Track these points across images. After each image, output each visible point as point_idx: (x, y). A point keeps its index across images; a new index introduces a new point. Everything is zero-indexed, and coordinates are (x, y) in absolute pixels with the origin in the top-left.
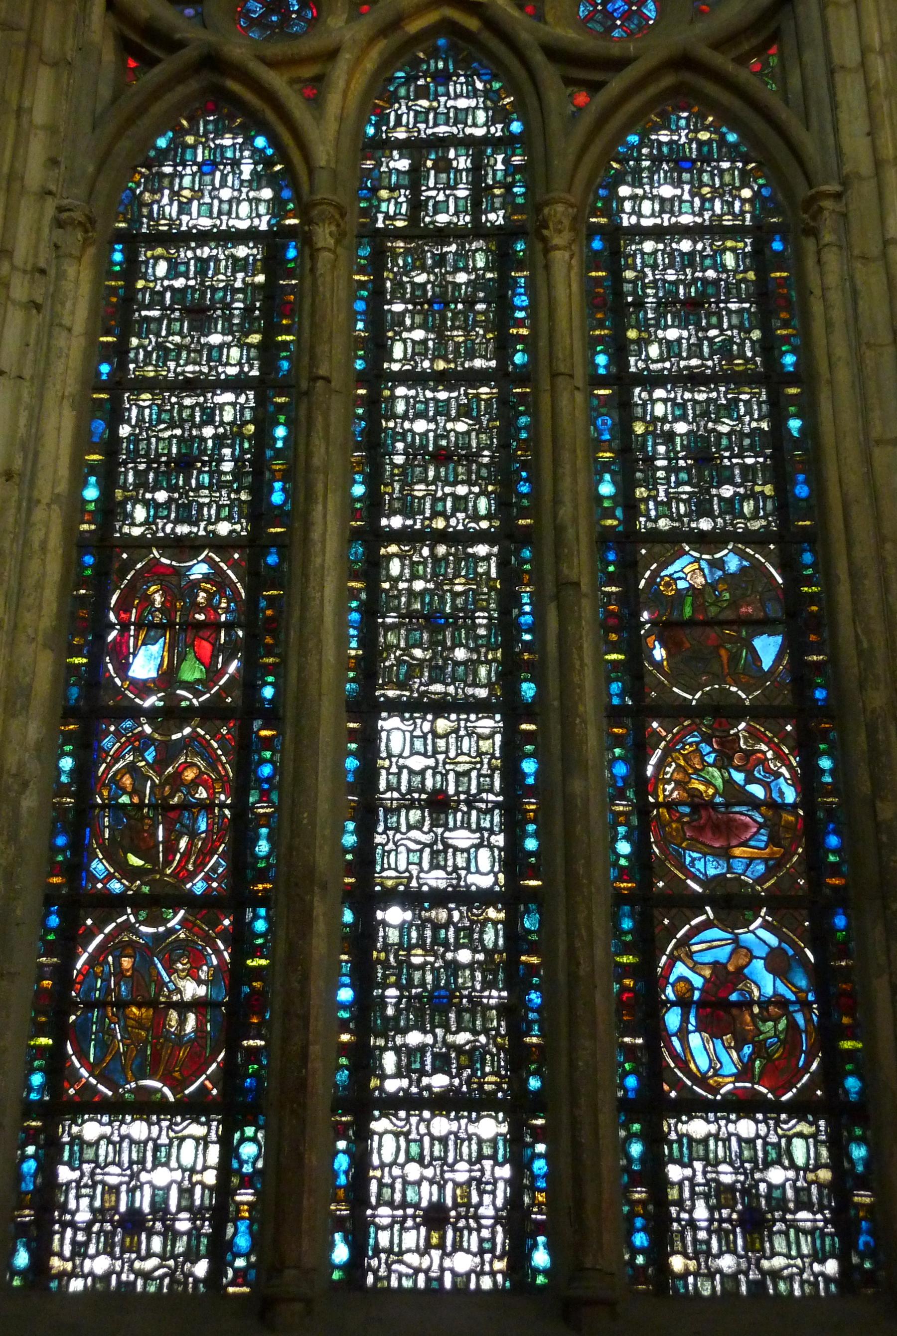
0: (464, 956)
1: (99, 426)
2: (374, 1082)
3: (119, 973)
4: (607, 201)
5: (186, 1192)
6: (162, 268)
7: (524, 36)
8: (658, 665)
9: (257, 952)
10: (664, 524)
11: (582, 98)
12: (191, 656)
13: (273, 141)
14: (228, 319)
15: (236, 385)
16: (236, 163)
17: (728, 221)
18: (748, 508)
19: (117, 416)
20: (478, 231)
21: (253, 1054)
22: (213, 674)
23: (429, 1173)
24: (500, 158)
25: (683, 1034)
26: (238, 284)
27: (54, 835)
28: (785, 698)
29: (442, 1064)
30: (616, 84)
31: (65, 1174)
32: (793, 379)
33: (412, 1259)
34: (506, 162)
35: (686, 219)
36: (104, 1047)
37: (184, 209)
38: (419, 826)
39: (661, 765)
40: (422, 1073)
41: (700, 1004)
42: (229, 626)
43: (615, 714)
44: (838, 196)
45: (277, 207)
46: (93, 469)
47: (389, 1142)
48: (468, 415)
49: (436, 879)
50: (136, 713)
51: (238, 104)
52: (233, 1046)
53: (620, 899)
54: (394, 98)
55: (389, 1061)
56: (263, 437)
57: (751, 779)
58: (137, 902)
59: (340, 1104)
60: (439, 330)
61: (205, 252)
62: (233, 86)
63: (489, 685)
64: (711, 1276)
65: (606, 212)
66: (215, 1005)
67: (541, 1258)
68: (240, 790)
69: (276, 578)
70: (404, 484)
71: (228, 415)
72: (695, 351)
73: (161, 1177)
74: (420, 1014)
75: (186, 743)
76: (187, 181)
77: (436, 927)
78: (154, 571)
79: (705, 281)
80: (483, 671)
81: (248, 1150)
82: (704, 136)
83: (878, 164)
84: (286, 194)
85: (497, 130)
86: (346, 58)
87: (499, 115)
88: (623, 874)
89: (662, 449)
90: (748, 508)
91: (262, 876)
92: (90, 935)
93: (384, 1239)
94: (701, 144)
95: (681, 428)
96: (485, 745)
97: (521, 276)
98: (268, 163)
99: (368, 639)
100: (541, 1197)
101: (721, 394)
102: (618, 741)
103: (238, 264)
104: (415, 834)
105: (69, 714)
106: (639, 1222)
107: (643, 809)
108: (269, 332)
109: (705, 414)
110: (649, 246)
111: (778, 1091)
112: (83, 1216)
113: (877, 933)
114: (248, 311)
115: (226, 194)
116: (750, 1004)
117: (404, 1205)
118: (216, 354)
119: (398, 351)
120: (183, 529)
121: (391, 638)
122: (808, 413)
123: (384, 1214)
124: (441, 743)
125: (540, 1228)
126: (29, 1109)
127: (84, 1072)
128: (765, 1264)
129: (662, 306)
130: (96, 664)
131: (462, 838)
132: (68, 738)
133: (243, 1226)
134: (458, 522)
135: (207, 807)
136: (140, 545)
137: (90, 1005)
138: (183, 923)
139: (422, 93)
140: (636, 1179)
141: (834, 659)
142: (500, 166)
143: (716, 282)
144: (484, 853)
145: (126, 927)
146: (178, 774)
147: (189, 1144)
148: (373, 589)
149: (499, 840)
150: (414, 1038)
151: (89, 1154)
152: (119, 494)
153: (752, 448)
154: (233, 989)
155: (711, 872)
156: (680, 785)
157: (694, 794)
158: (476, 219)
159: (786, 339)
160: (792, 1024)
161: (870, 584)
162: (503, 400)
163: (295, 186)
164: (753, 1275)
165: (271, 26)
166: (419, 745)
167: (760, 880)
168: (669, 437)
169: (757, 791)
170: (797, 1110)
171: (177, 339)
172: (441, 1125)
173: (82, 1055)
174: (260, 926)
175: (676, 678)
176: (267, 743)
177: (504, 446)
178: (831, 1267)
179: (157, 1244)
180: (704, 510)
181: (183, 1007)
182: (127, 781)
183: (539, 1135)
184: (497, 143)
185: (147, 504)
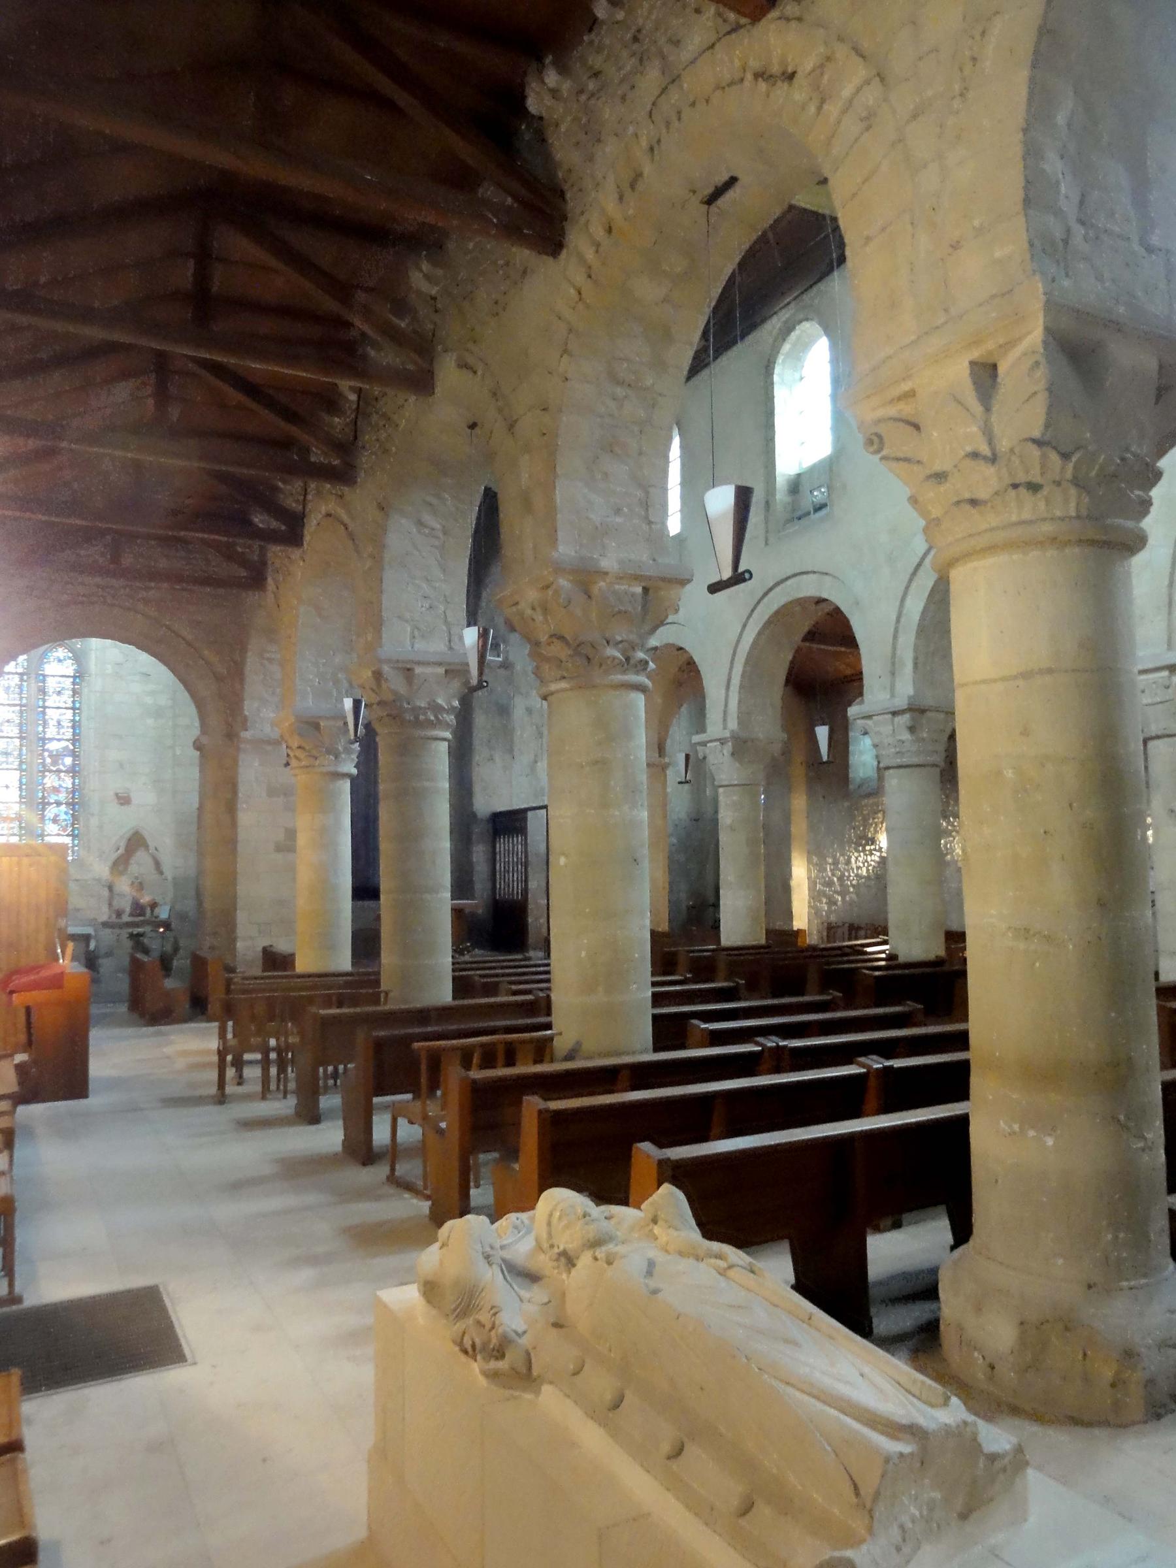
18: (66, 734)
20: (16, 673)
32: (78, 709)
43: (40, 772)
82: (66, 654)
101: (64, 711)
169: (64, 785)
170: (67, 835)
180: (59, 734)
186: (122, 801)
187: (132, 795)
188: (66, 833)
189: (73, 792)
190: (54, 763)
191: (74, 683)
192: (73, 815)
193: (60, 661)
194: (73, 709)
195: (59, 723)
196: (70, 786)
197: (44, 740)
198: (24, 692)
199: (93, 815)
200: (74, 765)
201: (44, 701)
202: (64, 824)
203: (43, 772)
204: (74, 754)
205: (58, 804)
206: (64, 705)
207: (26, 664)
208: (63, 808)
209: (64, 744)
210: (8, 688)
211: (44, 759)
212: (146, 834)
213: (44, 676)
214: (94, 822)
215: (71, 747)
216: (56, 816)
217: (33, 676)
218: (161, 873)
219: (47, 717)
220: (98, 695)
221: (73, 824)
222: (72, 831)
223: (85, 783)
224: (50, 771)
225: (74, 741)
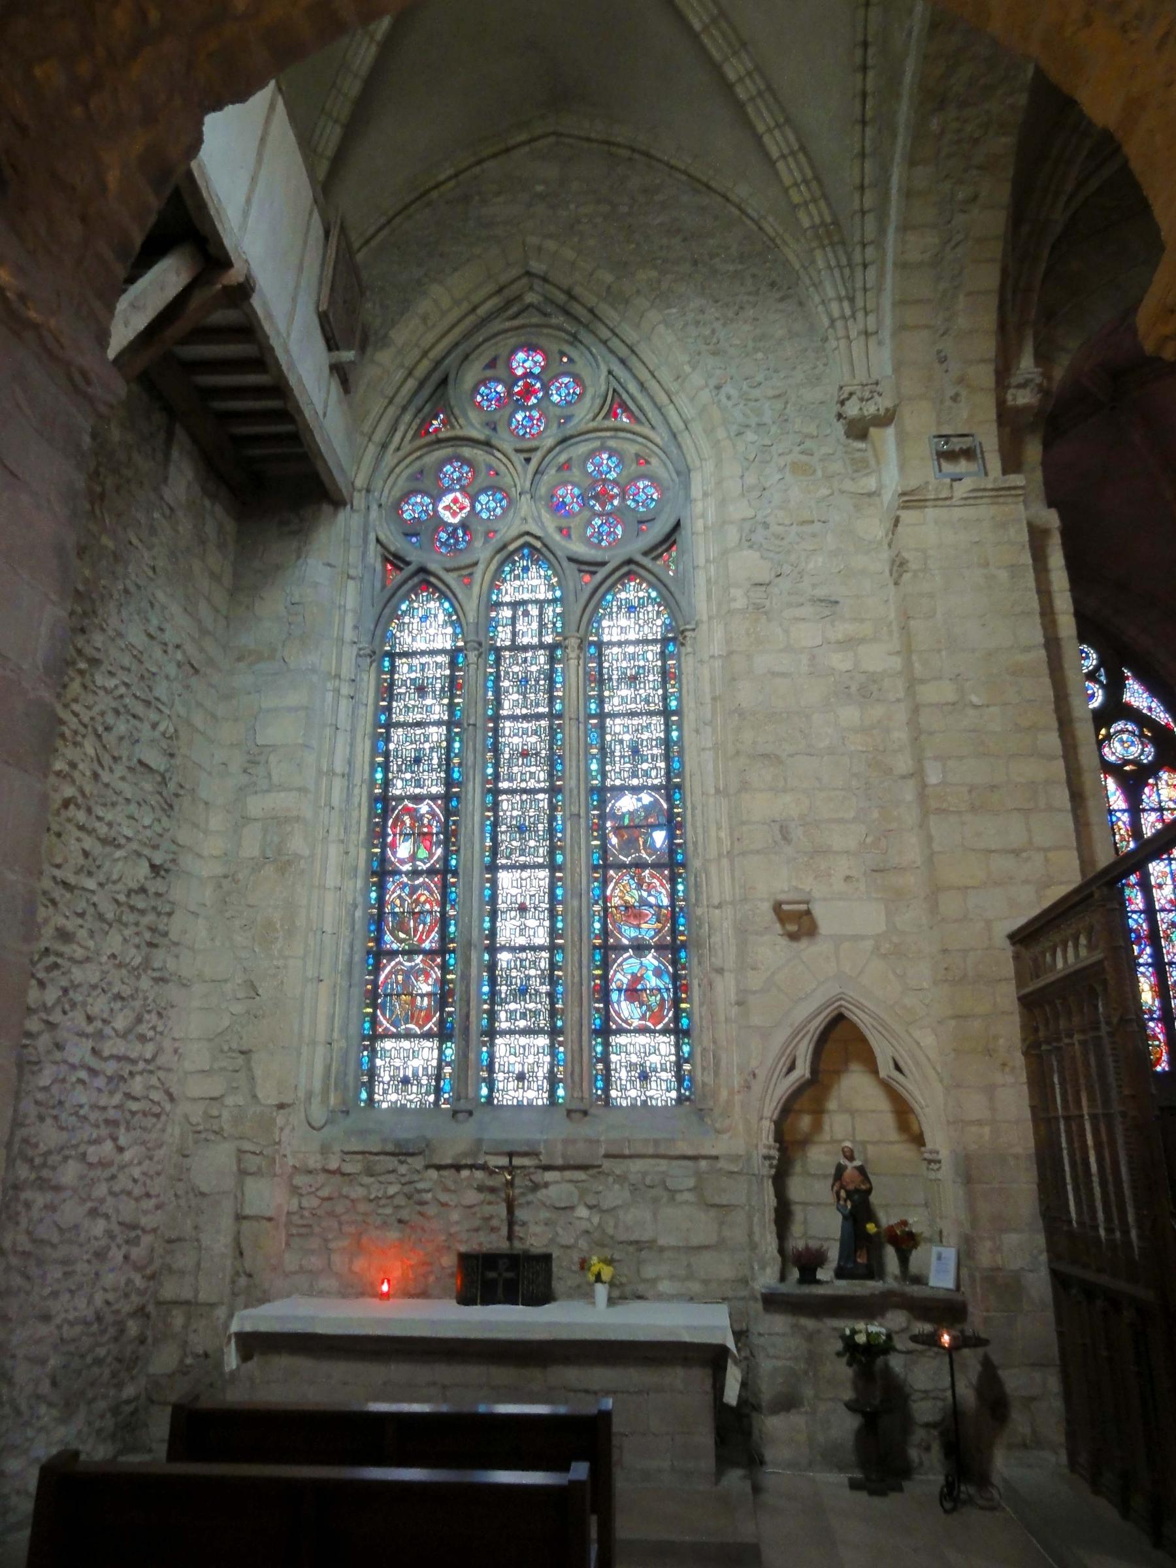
0: (532, 972)
1: (381, 744)
2: (497, 1024)
3: (397, 982)
4: (597, 629)
5: (425, 1069)
6: (405, 668)
7: (559, 553)
8: (614, 846)
9: (451, 972)
10: (618, 783)
11: (587, 577)
12: (422, 847)
13: (452, 605)
14: (434, 692)
15: (438, 723)
16: (436, 616)
17: (650, 637)
18: (654, 773)
19: (388, 740)
20: (541, 646)
21: (450, 1014)
22: (431, 855)
23: (518, 1059)
24: (551, 609)
25: (619, 1002)
26: (438, 675)
27: (369, 924)
28: (665, 859)
29: (523, 1016)
30: (602, 572)
31: (379, 1062)
32: (674, 713)
33: (512, 1093)
34: (554, 611)
35: (632, 636)
36: (392, 1012)
37: (414, 639)
38: (514, 918)
39: (614, 889)
40: (516, 1020)
41: (626, 990)
42: (437, 834)
43: (595, 868)
44: (693, 630)
45: (455, 636)
46: (379, 765)
47: (503, 1047)
48: (536, 734)
49: (521, 941)
50: (399, 873)
51: (436, 589)
52: (442, 1011)
53: (595, 947)
54: (504, 581)
55: (503, 1015)
56: (449, 749)
57: (649, 895)
58: (403, 953)
59: (484, 1033)
60: (524, 695)
61: (424, 660)
62: (432, 579)
63: (544, 857)
64: (626, 1098)
65: (597, 634)
66: (435, 994)
67: (561, 1092)
68: (443, 905)
69: (456, 813)
70: (509, 767)
71: (435, 738)
72: (634, 700)
73: (416, 1063)
74: (515, 996)
75: (420, 886)
76: (415, 626)
77: (521, 961)
78: (407, 810)
79: (639, 667)
80: (541, 850)
81: (448, 1052)
82: (641, 594)
83: (710, 618)
84: (458, 630)
85: (550, 596)
86: (481, 566)
87: (551, 588)
88: (597, 937)
89: (618, 747)
90: (654, 773)
91: (452, 941)
92: (385, 966)
93: (501, 1086)
94: (639, 599)
95: (627, 737)
96: (542, 883)
97: (559, 667)
98: (450, 616)
99: (494, 839)
100: (561, 1068)
101: (644, 721)
102: (596, 879)
103: (438, 666)
104: (513, 922)
105: (374, 873)
106: (599, 1077)
107: (605, 909)
108: (452, 697)
109: (637, 730)
110: (615, 650)
111: (655, 1025)
112: (387, 1079)
113: (695, 961)
114: (443, 688)
115: (432, 631)
116: (645, 990)
117: (509, 1072)
118: (429, 709)
119: (506, 704)
120: (417, 791)
121: (504, 837)
122: (680, 729)
123: (500, 1076)
124: (524, 883)
125: (561, 1080)
126: (364, 1038)
127: (385, 1022)
128: (648, 1094)
129: (619, 680)
130: (383, 852)
131: (531, 923)
132: (374, 884)
133: (447, 1081)
134: (532, 784)
135: (431, 912)
136: (400, 799)
137: (386, 995)
138: (422, 961)
139: (517, 577)
140: (599, 1061)
141: (685, 843)
142: (551, 614)
143: (644, 667)
144: (541, 929)
145: (400, 963)
146: (418, 899)
147: (426, 1050)
148: (496, 816)
149: (547, 923)
150: (513, 1006)
151: (388, 1054)
152: (390, 775)
153: (656, 746)
154: (442, 988)
155: (633, 935)
156: (621, 898)
157: (626, 902)
158: (540, 640)
159: (672, 694)
160: (662, 999)
161: (698, 812)
162: (551, 727)
163: (461, 626)
164: (643, 1098)
165: (450, 546)
166: (515, 884)
167: (652, 938)
168: (621, 742)
169: (652, 900)
170: (665, 1032)
171: (412, 702)
172: (523, 1040)
173: (384, 1015)
174: (452, 961)
175: (620, 850)
176: (454, 884)
177: (551, 748)
178: (674, 1094)
179: (415, 1089)
180: (634, 775)
181: (422, 996)
182: (398, 902)
183: (561, 1044)
184: (549, 602)
185: (402, 779)
186: (793, 928)
187: (818, 911)
188: (659, 1027)
189: (674, 918)
190: (629, 845)
191: (663, 656)
192: (675, 978)
193: (631, 609)
194: (666, 713)
195: (635, 751)
196: (666, 902)
197: (603, 793)
198: (558, 686)
199: (720, 971)
200: (672, 849)
201: (601, 701)
202: (654, 1000)
203: (606, 867)
204: (672, 824)
205: (640, 948)
206: (641, 706)
207: (559, 625)
208: (650, 960)
209: (646, 798)
210: (526, 680)
211: (604, 838)
212: (860, 1018)
213: (599, 645)
214: (726, 988)
215: (665, 806)
216: (636, 979)
217: (573, 642)
218: (918, 1140)
219: (608, 738)
220: (717, 663)
221: (676, 1002)
222: (677, 1019)
223: (697, 885)
224: (620, 866)
225: (670, 789)
